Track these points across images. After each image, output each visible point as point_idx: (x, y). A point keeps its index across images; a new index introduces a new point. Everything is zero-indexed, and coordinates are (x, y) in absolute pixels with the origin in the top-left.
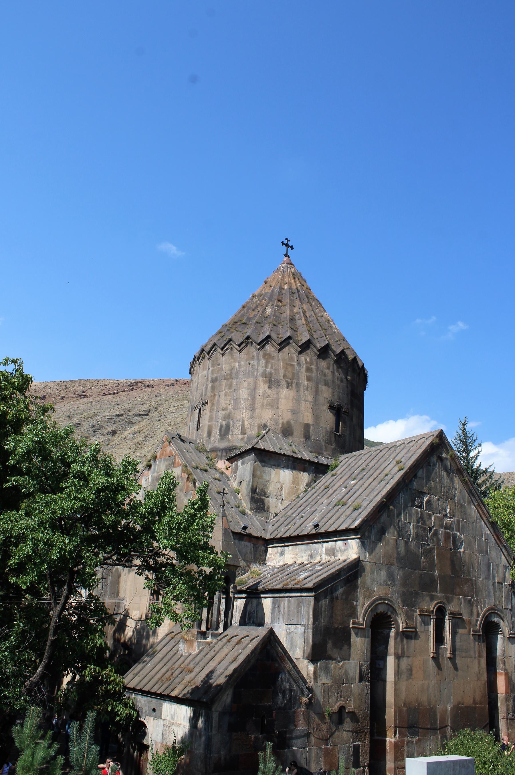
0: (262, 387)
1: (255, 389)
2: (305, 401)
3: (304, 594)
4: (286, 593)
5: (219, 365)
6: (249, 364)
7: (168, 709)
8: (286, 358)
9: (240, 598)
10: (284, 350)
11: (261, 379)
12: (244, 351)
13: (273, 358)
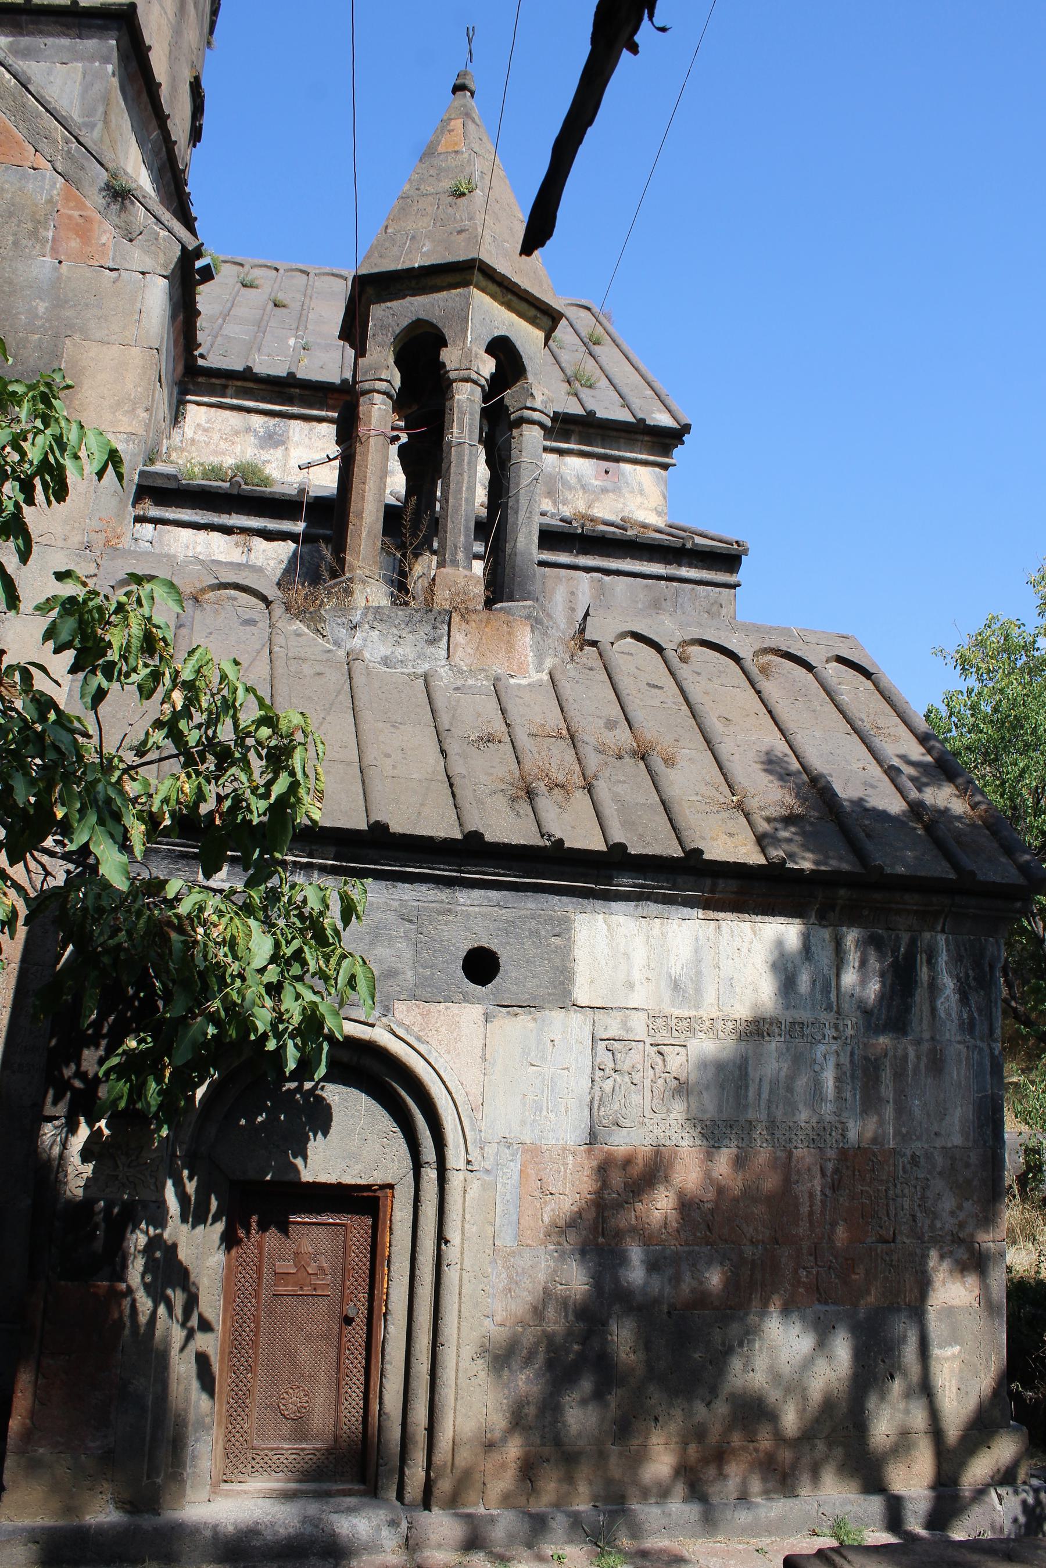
3: (685, 572)
4: (585, 552)
7: (621, 949)
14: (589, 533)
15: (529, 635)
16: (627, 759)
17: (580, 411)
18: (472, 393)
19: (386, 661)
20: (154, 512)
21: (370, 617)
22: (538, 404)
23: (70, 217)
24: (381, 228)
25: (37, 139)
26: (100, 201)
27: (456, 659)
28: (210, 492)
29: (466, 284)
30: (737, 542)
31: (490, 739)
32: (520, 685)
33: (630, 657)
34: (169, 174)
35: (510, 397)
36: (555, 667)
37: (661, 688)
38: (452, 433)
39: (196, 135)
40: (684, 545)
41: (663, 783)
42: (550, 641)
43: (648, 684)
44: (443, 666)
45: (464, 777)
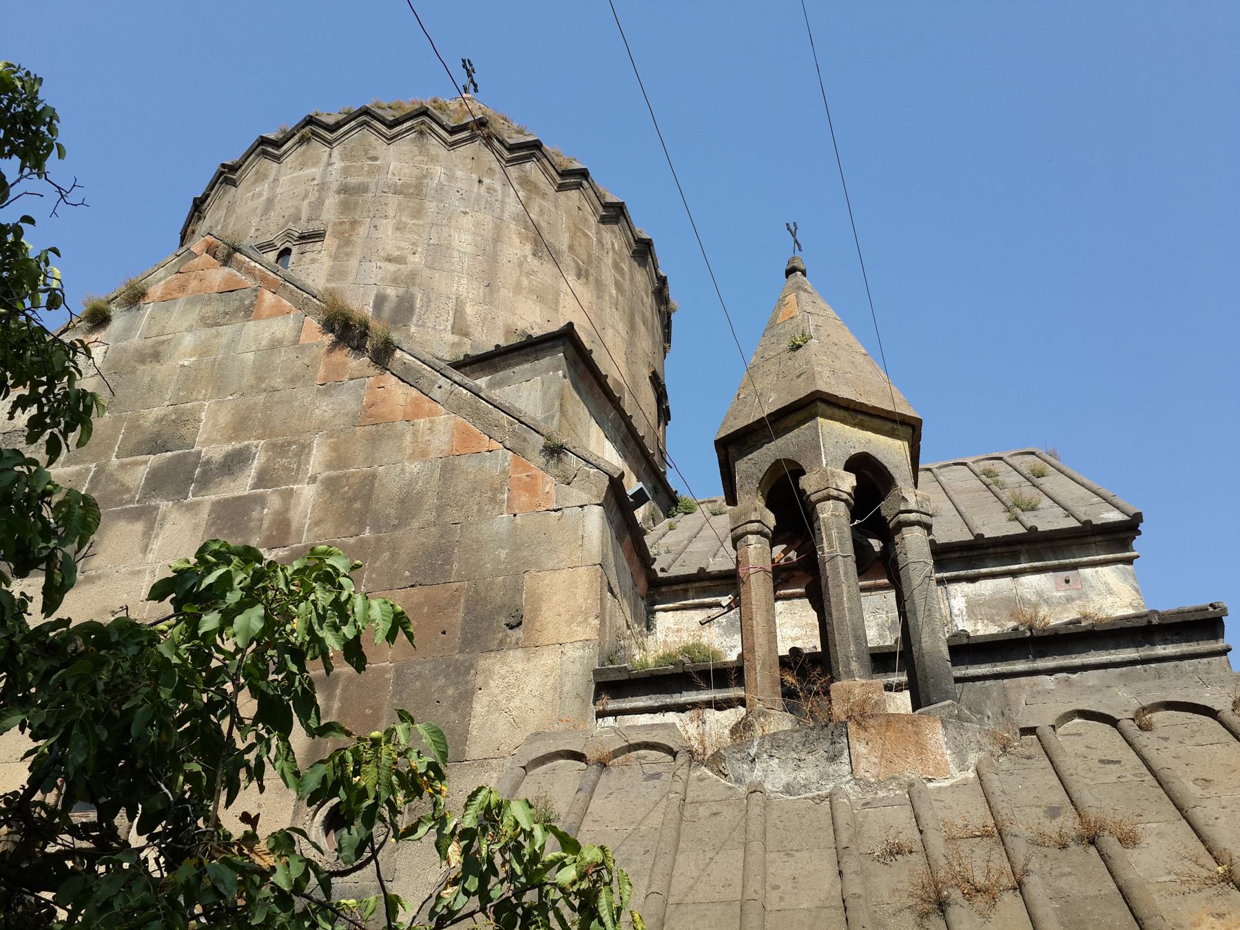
0: (516, 248)
1: (497, 240)
2: (613, 327)
3: (1160, 650)
4: (1042, 655)
5: (375, 159)
6: (480, 181)
8: (575, 212)
9: (720, 705)
10: (569, 193)
11: (513, 226)
12: (466, 150)
13: (544, 196)
14: (1040, 634)
15: (941, 731)
16: (1073, 847)
17: (1022, 530)
18: (835, 509)
19: (788, 789)
20: (613, 705)
21: (767, 746)
22: (912, 505)
23: (519, 479)
24: (734, 399)
25: (490, 430)
26: (542, 460)
27: (861, 773)
28: (664, 676)
29: (813, 417)
30: (1211, 605)
31: (896, 851)
32: (940, 788)
33: (1077, 738)
34: (633, 443)
35: (886, 508)
36: (980, 761)
37: (1119, 762)
38: (822, 549)
39: (664, 415)
40: (1150, 622)
41: (1118, 866)
42: (970, 734)
43: (1102, 761)
44: (848, 782)
45: (859, 897)
